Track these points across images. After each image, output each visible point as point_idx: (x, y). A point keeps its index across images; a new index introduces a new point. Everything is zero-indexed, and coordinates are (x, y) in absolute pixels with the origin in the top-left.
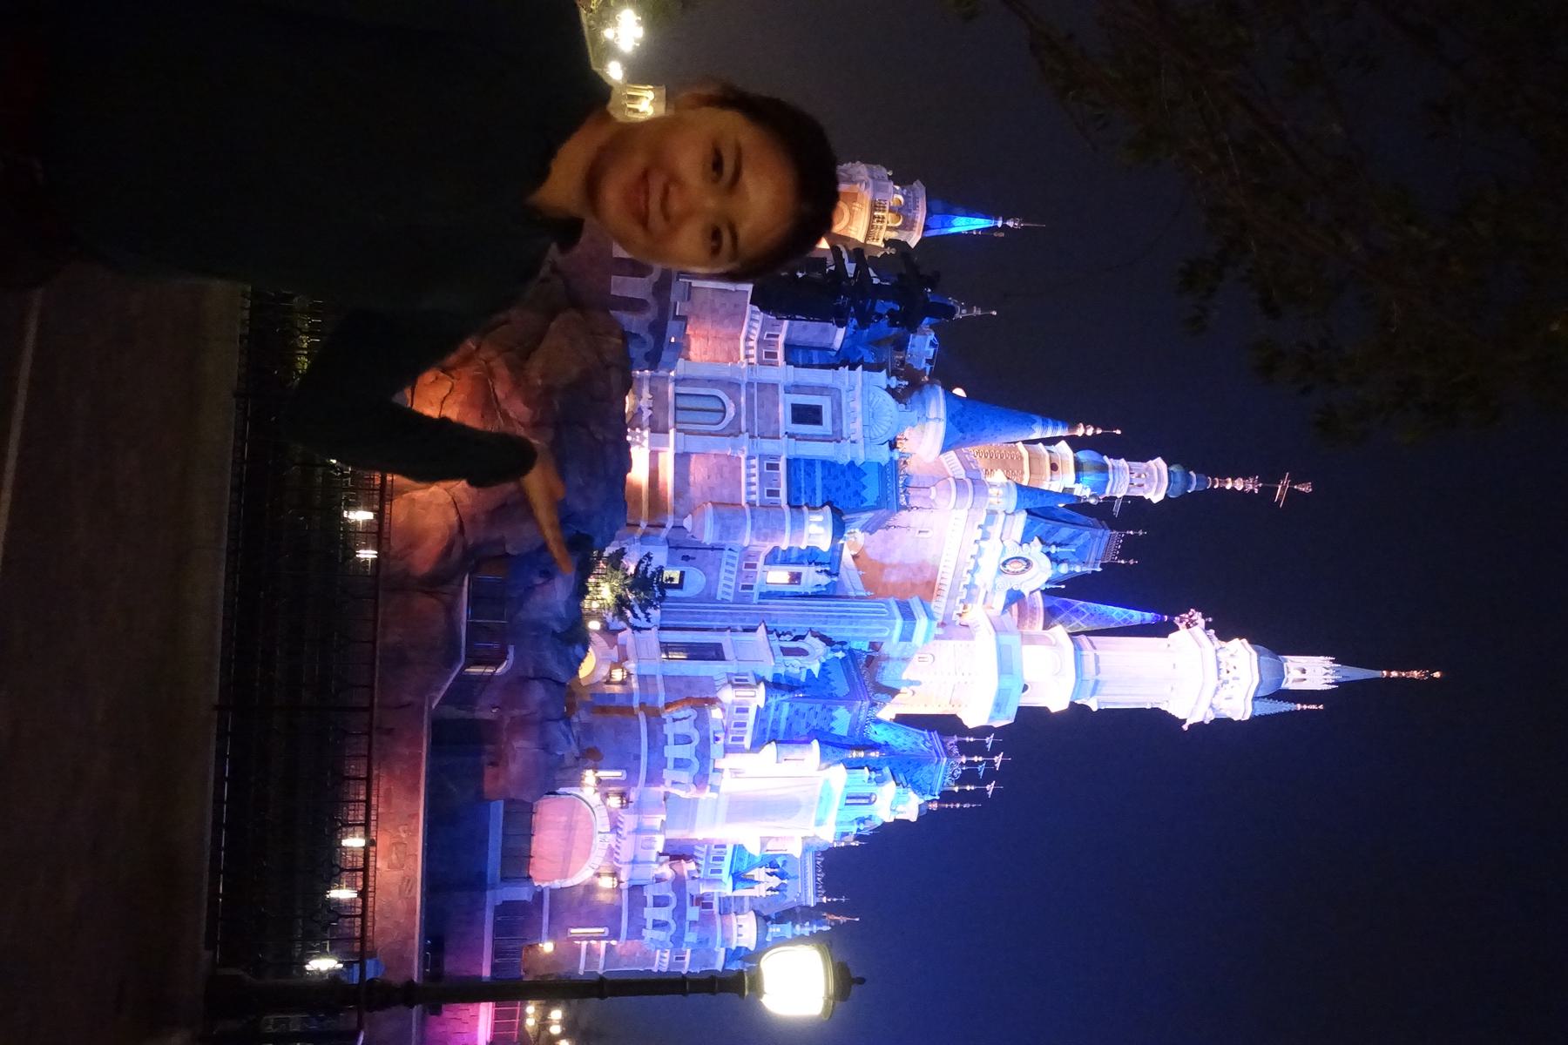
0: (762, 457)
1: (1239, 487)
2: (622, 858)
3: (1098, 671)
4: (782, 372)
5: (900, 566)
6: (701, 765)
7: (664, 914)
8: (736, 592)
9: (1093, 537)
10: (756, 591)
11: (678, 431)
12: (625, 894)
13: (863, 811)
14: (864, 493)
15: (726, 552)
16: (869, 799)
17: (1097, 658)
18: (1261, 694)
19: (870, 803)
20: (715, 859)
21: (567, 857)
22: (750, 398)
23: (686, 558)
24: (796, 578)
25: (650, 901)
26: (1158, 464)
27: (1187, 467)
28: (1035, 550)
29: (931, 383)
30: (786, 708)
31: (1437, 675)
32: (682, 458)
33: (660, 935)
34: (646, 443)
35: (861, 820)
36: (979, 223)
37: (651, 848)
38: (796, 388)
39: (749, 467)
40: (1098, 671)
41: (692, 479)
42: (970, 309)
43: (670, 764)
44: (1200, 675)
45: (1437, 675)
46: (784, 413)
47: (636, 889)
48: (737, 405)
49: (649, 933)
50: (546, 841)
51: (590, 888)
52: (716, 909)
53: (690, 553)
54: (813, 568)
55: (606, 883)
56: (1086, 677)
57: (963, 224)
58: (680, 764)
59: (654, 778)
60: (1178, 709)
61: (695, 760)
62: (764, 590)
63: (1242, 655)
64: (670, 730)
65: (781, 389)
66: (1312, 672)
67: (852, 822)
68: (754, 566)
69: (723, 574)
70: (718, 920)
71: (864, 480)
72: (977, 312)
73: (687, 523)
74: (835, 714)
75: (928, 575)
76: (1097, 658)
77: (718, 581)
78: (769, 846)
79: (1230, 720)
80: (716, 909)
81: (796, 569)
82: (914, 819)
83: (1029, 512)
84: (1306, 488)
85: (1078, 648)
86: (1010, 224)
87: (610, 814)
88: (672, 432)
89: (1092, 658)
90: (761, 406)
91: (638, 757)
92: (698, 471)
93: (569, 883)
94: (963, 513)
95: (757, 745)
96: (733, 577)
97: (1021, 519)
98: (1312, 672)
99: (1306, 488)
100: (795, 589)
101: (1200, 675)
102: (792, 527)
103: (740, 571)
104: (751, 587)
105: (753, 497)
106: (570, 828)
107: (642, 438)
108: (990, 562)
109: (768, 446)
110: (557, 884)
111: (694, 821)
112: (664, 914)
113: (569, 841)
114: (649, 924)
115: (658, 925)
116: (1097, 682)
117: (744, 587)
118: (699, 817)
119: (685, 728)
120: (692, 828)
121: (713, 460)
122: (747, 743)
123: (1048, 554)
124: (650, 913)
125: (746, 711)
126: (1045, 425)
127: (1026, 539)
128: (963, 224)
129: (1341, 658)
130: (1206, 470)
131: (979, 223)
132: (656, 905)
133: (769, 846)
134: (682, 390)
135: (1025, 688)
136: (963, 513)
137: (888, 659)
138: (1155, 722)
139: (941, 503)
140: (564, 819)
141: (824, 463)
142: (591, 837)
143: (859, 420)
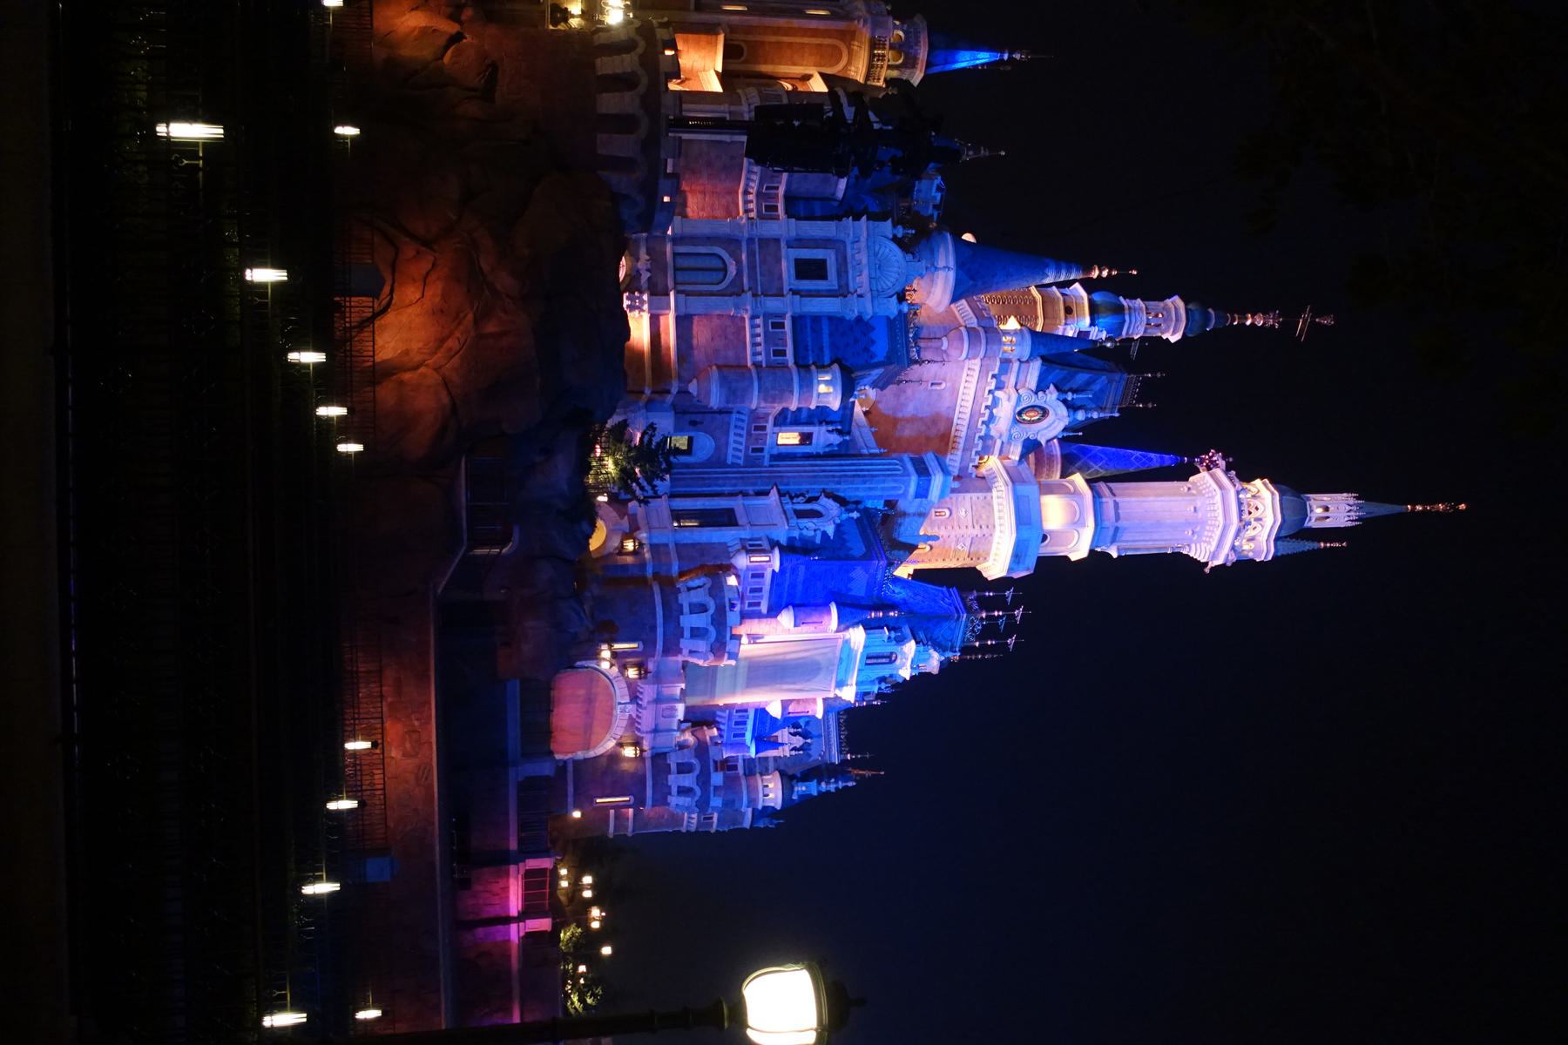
0: (767, 316)
2: (644, 728)
3: (1118, 517)
4: (783, 226)
5: (913, 420)
6: (718, 633)
7: (688, 780)
8: (746, 456)
9: (1110, 382)
10: (766, 454)
11: (678, 293)
12: (648, 763)
13: (885, 671)
14: (873, 349)
15: (734, 416)
16: (890, 659)
17: (1116, 504)
18: (1283, 534)
19: (891, 662)
20: (737, 723)
22: (751, 254)
23: (693, 423)
24: (806, 438)
25: (674, 767)
26: (1176, 303)
27: (1205, 305)
28: (1051, 397)
29: (939, 230)
30: (802, 569)
31: (1463, 506)
32: (683, 322)
33: (685, 801)
34: (646, 307)
35: (882, 680)
36: (983, 58)
37: (673, 716)
38: (799, 242)
39: (753, 327)
40: (1118, 517)
41: (695, 342)
42: (977, 151)
43: (687, 633)
44: (1222, 517)
45: (1463, 506)
46: (786, 268)
47: (659, 758)
48: (739, 262)
49: (674, 800)
50: (567, 715)
51: (614, 757)
52: (740, 771)
53: (694, 417)
54: (824, 428)
55: (629, 752)
56: (1106, 523)
57: (967, 60)
58: (697, 633)
59: (671, 648)
60: (1199, 553)
62: (775, 452)
63: (1264, 495)
64: (685, 599)
65: (783, 244)
66: (1334, 510)
67: (872, 682)
68: (764, 428)
69: (732, 438)
70: (743, 782)
71: (873, 335)
73: (693, 387)
74: (853, 575)
75: (942, 427)
76: (1116, 504)
77: (727, 443)
78: (791, 709)
79: (1252, 561)
80: (740, 771)
81: (807, 429)
82: (935, 671)
83: (1044, 359)
85: (1097, 496)
86: (1017, 56)
88: (672, 294)
89: (1111, 505)
90: (763, 262)
91: (654, 628)
92: (701, 334)
93: (592, 754)
94: (976, 364)
95: (774, 612)
96: (743, 440)
97: (1035, 368)
98: (1334, 510)
100: (806, 449)
101: (1222, 517)
102: (801, 387)
103: (749, 434)
104: (761, 450)
105: (759, 358)
106: (590, 700)
107: (642, 302)
108: (1005, 411)
109: (772, 304)
110: (580, 755)
111: (714, 685)
112: (688, 780)
113: (589, 714)
114: (674, 791)
115: (683, 791)
116: (1117, 529)
117: (754, 450)
119: (699, 596)
120: (713, 695)
121: (716, 321)
122: (764, 608)
123: (1065, 402)
124: (674, 780)
125: (762, 576)
127: (1041, 387)
128: (967, 60)
129: (1364, 493)
131: (983, 58)
132: (679, 772)
133: (791, 709)
135: (1044, 538)
136: (976, 364)
137: (904, 514)
138: (1178, 565)
140: (582, 692)
142: (612, 708)
143: (866, 272)
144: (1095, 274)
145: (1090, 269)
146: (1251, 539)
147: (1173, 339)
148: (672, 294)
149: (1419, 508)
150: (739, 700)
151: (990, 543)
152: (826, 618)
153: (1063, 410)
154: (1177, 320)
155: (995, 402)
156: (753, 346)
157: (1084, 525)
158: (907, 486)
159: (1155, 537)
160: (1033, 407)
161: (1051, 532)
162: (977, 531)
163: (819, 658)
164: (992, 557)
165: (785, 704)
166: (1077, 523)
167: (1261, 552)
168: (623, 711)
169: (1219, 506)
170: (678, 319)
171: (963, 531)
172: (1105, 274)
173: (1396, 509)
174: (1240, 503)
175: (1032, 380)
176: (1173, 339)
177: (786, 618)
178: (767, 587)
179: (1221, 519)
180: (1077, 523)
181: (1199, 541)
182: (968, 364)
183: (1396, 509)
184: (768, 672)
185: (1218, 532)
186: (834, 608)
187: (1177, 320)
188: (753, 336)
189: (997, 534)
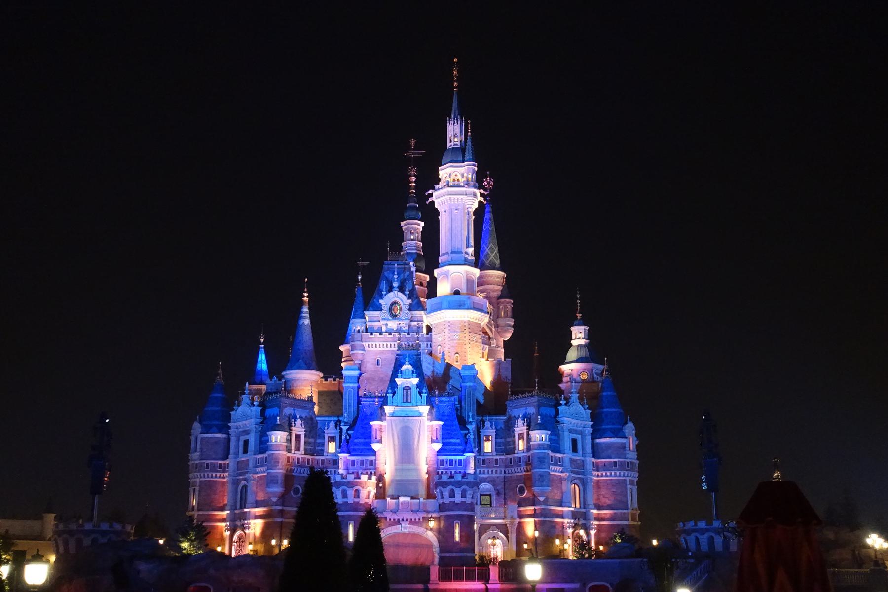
1: (414, 179)
4: (230, 462)
9: (388, 269)
11: (245, 507)
13: (415, 391)
16: (407, 389)
18: (461, 159)
21: (416, 546)
24: (332, 439)
27: (406, 208)
28: (385, 302)
29: (281, 378)
30: (356, 441)
32: (257, 504)
33: (469, 493)
35: (420, 393)
36: (262, 357)
39: (259, 472)
40: (447, 253)
42: (218, 375)
43: (345, 500)
44: (457, 194)
46: (243, 458)
49: (468, 500)
51: (439, 532)
61: (341, 488)
63: (446, 172)
65: (238, 460)
68: (323, 461)
72: (220, 371)
73: (275, 499)
80: (529, 454)
82: (573, 328)
84: (413, 141)
87: (391, 525)
88: (246, 510)
92: (261, 496)
95: (374, 453)
97: (368, 314)
98: (455, 133)
99: (413, 141)
101: (457, 194)
106: (397, 546)
108: (393, 324)
109: (251, 464)
110: (436, 549)
111: (407, 480)
112: (446, 492)
113: (405, 546)
114: (463, 500)
115: (452, 495)
116: (453, 252)
118: (410, 478)
120: (418, 481)
122: (373, 458)
124: (447, 500)
125: (353, 461)
126: (301, 318)
127: (379, 308)
130: (406, 198)
131: (262, 357)
133: (434, 438)
134: (238, 507)
135: (457, 293)
136: (366, 345)
137: (433, 372)
139: (360, 357)
141: (261, 436)
142: (404, 534)
144: (306, 299)
146: (463, 176)
147: (422, 224)
148: (246, 510)
149: (455, 84)
150: (424, 468)
151: (454, 321)
152: (374, 428)
153: (391, 294)
154: (408, 224)
156: (262, 472)
157: (448, 271)
158: (349, 387)
159: (459, 229)
160: (390, 309)
161: (452, 289)
162: (447, 330)
163: (399, 427)
164: (466, 319)
165: (433, 441)
166: (446, 275)
167: (473, 170)
168: (406, 528)
169: (441, 199)
170: (256, 507)
171: (447, 338)
172: (306, 294)
173: (455, 97)
174: (454, 186)
176: (422, 224)
177: (375, 446)
178: (360, 458)
179: (447, 197)
180: (446, 275)
181: (464, 205)
182: (366, 348)
183: (455, 97)
184: (406, 451)
186: (371, 423)
187: (408, 224)
188: (262, 472)
189: (448, 319)
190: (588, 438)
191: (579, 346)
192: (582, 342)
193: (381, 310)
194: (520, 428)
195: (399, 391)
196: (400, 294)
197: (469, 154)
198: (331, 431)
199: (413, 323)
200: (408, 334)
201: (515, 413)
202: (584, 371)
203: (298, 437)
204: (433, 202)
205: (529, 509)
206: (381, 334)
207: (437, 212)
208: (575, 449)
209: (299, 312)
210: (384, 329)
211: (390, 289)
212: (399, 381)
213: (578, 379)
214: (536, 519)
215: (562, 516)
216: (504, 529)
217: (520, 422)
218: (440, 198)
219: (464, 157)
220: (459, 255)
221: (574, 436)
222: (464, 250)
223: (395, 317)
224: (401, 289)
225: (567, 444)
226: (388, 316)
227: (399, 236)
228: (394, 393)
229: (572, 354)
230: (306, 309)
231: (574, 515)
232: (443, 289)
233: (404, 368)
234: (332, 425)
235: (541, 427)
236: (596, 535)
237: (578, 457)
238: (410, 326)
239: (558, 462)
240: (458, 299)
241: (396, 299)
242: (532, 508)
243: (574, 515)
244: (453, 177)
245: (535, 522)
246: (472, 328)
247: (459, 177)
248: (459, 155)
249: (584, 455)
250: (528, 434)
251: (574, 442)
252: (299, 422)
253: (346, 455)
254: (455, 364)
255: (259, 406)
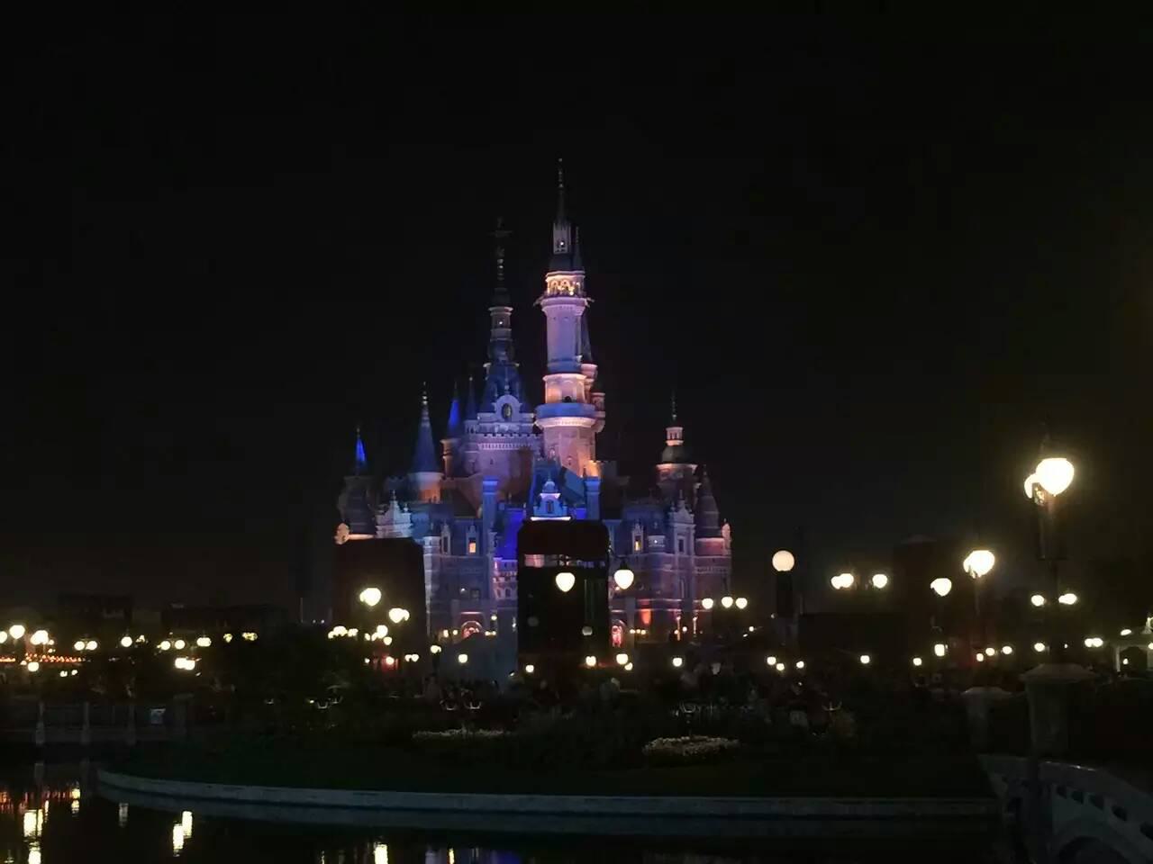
1: (501, 261)
5: (511, 470)
13: (557, 504)
16: (550, 503)
24: (472, 540)
28: (497, 405)
35: (561, 505)
36: (360, 447)
52: (646, 555)
57: (361, 455)
60: (579, 311)
81: (468, 541)
83: (478, 411)
84: (500, 221)
94: (480, 445)
97: (480, 416)
98: (561, 238)
100: (477, 540)
108: (505, 426)
123: (498, 398)
125: (506, 565)
128: (361, 455)
131: (360, 447)
136: (480, 445)
138: (590, 316)
145: (424, 406)
146: (571, 284)
153: (503, 398)
155: (502, 433)
157: (560, 378)
166: (558, 382)
175: (489, 415)
180: (558, 382)
185: (563, 306)
190: (692, 538)
191: (675, 447)
192: (678, 442)
193: (494, 412)
194: (637, 531)
195: (543, 505)
196: (511, 397)
197: (578, 259)
198: (472, 533)
199: (524, 425)
200: (520, 435)
201: (630, 517)
202: (678, 471)
203: (446, 539)
204: (540, 307)
205: (646, 601)
206: (494, 435)
207: (544, 317)
208: (681, 549)
209: (419, 418)
210: (496, 430)
211: (501, 393)
212: (543, 495)
213: (674, 478)
214: (653, 610)
215: (671, 606)
216: (623, 617)
217: (638, 526)
218: (549, 307)
219: (572, 265)
220: (568, 362)
221: (681, 537)
222: (574, 357)
223: (507, 419)
224: (512, 392)
225: (676, 546)
226: (500, 418)
227: (488, 322)
228: (539, 505)
229: (668, 454)
230: (426, 413)
231: (681, 606)
232: (552, 393)
233: (548, 483)
234: (472, 528)
235: (657, 533)
236: (697, 621)
237: (685, 555)
238: (521, 427)
239: (670, 560)
240: (569, 404)
241: (505, 402)
242: (649, 600)
243: (681, 606)
244: (562, 283)
245: (652, 612)
246: (582, 431)
247: (568, 285)
248: (566, 264)
249: (689, 553)
250: (645, 537)
251: (681, 542)
252: (446, 527)
253: (500, 559)
254: (569, 467)
255: (409, 511)
